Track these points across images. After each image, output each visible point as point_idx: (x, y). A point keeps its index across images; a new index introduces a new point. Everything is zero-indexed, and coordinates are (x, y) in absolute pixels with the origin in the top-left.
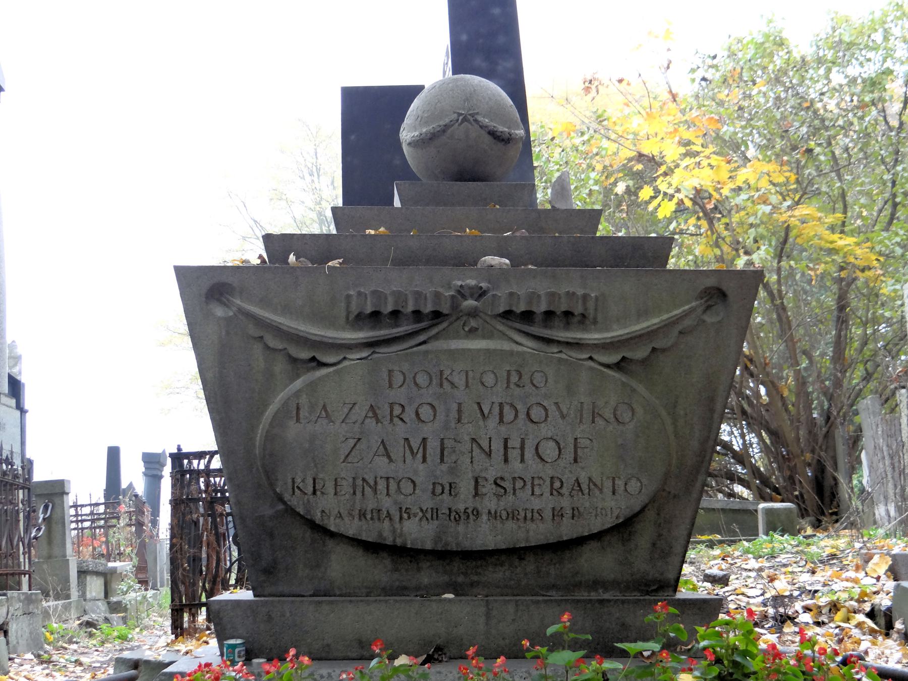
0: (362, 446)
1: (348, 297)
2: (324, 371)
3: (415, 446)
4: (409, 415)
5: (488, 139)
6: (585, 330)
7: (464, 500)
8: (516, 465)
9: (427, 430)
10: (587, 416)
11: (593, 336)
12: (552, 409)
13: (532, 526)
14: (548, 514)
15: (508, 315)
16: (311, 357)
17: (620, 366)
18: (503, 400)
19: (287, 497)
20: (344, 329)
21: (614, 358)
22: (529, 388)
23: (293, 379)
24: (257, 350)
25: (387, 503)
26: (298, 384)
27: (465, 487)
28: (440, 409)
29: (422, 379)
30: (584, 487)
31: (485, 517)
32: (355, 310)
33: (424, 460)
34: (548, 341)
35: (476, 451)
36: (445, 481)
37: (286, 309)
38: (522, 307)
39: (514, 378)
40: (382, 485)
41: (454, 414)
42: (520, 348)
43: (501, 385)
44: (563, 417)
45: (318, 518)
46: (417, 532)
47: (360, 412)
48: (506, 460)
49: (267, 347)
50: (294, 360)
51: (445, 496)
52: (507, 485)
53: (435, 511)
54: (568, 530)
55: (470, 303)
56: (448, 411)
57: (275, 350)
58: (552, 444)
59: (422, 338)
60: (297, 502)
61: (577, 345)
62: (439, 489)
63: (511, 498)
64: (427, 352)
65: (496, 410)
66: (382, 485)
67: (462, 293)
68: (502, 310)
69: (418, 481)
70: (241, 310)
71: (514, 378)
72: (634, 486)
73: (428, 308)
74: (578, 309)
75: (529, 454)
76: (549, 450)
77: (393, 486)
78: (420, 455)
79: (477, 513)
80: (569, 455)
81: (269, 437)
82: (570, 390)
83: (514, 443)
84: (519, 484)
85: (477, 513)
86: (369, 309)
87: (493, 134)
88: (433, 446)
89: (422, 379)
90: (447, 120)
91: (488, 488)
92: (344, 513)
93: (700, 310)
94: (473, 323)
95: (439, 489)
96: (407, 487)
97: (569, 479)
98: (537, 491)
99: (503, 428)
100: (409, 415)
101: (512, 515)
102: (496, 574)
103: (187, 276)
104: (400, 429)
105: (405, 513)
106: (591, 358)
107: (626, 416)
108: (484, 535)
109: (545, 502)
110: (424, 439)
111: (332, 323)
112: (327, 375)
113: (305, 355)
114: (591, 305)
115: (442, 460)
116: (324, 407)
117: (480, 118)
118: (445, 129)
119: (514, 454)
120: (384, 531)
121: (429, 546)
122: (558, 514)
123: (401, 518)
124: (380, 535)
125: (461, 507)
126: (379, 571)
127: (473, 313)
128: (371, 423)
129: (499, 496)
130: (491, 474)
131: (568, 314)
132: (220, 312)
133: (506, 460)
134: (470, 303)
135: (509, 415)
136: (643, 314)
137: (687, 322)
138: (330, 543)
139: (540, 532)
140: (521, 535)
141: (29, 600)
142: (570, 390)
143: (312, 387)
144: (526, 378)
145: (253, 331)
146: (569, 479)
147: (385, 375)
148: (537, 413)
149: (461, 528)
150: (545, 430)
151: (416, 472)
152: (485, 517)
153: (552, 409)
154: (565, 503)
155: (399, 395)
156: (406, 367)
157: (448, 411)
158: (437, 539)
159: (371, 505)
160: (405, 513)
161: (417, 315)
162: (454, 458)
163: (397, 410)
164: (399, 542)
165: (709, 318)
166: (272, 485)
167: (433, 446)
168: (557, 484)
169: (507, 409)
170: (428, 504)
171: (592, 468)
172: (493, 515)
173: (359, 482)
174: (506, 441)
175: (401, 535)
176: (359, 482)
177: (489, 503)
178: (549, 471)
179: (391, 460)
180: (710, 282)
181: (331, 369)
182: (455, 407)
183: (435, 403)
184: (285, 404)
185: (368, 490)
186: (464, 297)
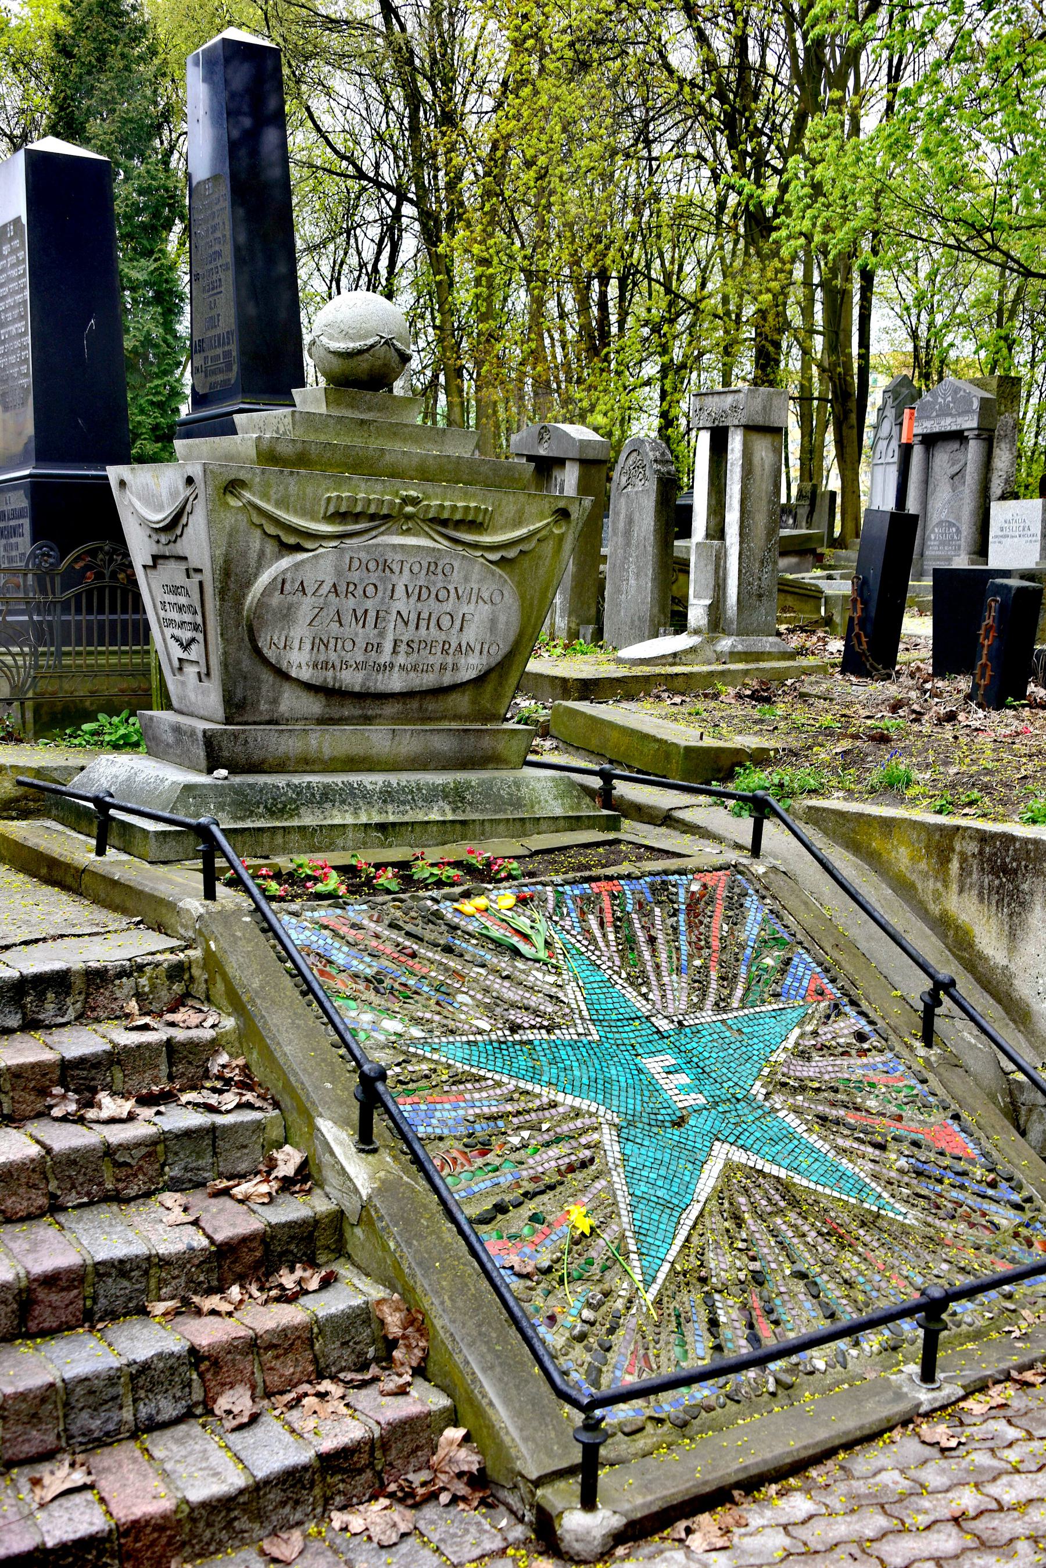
0: (323, 613)
4: (359, 592)
7: (386, 657)
8: (423, 630)
9: (369, 604)
10: (474, 598)
11: (487, 539)
12: (452, 591)
13: (425, 675)
14: (437, 667)
15: (432, 520)
17: (503, 562)
19: (265, 651)
22: (440, 576)
23: (277, 559)
24: (258, 533)
25: (333, 657)
27: (388, 646)
29: (372, 565)
32: (331, 510)
40: (332, 645)
45: (284, 666)
46: (352, 679)
52: (415, 646)
54: (447, 679)
55: (409, 509)
60: (270, 654)
61: (475, 546)
66: (332, 641)
67: (406, 501)
72: (494, 649)
76: (446, 621)
81: (260, 604)
82: (466, 579)
83: (425, 615)
85: (392, 665)
86: (343, 510)
88: (371, 615)
89: (372, 565)
90: (370, 341)
91: (403, 648)
96: (349, 645)
101: (415, 668)
102: (390, 709)
104: (351, 603)
107: (497, 598)
108: (396, 683)
109: (436, 659)
111: (313, 519)
113: (292, 540)
119: (423, 624)
120: (328, 677)
121: (357, 689)
122: (443, 667)
125: (382, 661)
126: (314, 706)
127: (409, 517)
128: (332, 596)
132: (233, 502)
134: (409, 509)
135: (424, 596)
136: (517, 523)
137: (543, 533)
138: (287, 687)
139: (428, 680)
140: (418, 681)
142: (466, 579)
143: (297, 566)
145: (256, 519)
148: (443, 594)
149: (380, 677)
150: (448, 607)
153: (452, 591)
155: (355, 576)
156: (363, 555)
158: (363, 684)
159: (322, 658)
161: (373, 517)
163: (351, 588)
166: (253, 640)
167: (371, 615)
170: (360, 658)
171: (470, 635)
172: (402, 668)
177: (401, 659)
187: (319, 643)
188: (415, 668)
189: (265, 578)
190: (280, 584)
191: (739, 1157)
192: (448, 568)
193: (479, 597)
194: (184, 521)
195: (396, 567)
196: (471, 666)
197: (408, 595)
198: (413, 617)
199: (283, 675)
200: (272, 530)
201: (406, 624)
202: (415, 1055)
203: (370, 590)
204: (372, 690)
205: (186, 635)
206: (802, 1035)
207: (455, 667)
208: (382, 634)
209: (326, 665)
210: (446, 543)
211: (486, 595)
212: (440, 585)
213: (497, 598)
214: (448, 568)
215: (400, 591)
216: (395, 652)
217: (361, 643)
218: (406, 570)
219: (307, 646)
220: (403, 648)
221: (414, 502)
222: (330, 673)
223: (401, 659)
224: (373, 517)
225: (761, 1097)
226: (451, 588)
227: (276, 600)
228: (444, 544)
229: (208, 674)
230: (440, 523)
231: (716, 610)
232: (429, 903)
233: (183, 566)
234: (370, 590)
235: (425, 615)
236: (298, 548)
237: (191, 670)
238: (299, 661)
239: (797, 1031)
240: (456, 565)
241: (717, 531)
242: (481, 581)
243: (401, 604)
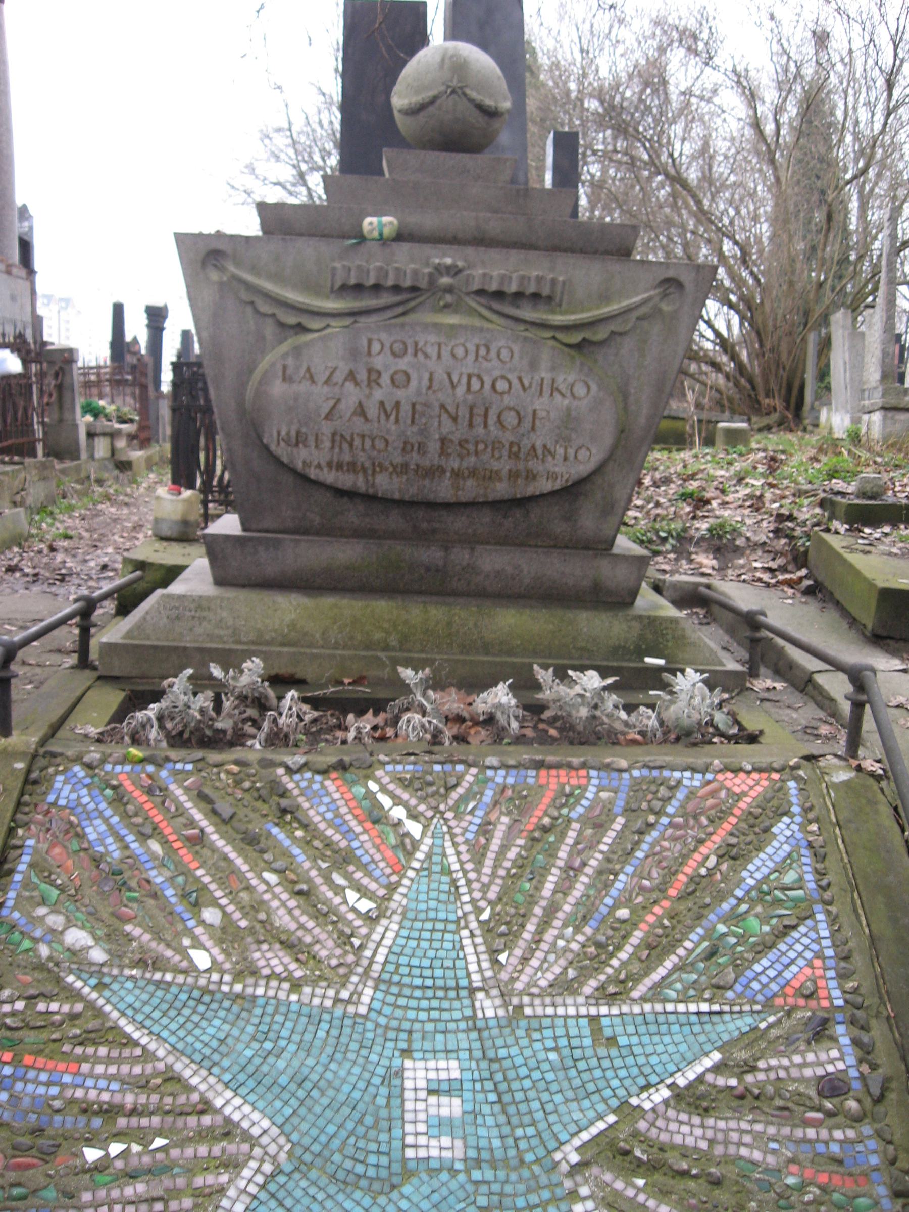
1: (334, 269)
2: (310, 337)
3: (389, 408)
5: (476, 113)
6: (553, 312)
9: (400, 394)
11: (558, 319)
14: (504, 473)
15: (481, 292)
16: (295, 324)
17: (578, 347)
18: (470, 371)
19: (273, 448)
20: (328, 298)
22: (495, 362)
25: (362, 458)
26: (284, 347)
27: (434, 447)
28: (414, 376)
30: (540, 452)
31: (448, 474)
32: (338, 284)
33: (397, 421)
35: (445, 416)
36: (414, 440)
37: (277, 277)
38: (494, 287)
39: (483, 351)
40: (357, 442)
41: (425, 382)
42: (490, 326)
43: (471, 357)
44: (524, 389)
45: (299, 466)
47: (339, 377)
48: (471, 425)
49: (256, 311)
50: (282, 325)
51: (414, 454)
52: (471, 447)
53: (405, 466)
55: (445, 280)
56: (420, 379)
57: (265, 315)
58: (513, 413)
59: (400, 310)
61: (544, 326)
62: (409, 448)
63: (473, 459)
64: (403, 325)
65: (464, 380)
67: (442, 270)
68: (475, 287)
69: (391, 439)
70: (235, 277)
71: (483, 351)
73: (407, 283)
74: (546, 292)
77: (368, 443)
78: (393, 417)
80: (527, 424)
82: (533, 365)
83: (479, 411)
84: (481, 447)
85: (443, 471)
86: (353, 281)
87: (480, 107)
88: (406, 408)
92: (323, 463)
93: (657, 299)
94: (449, 298)
95: (409, 448)
96: (380, 445)
98: (497, 454)
99: (470, 397)
103: (184, 241)
106: (554, 338)
107: (580, 390)
112: (312, 341)
113: (292, 320)
114: (559, 288)
115: (413, 422)
116: (308, 370)
117: (468, 91)
118: (433, 101)
119: (478, 420)
121: (397, 496)
122: (514, 475)
123: (374, 471)
124: (355, 484)
127: (449, 290)
128: (349, 386)
129: (462, 457)
130: (456, 437)
131: (536, 296)
132: (214, 276)
133: (471, 425)
141: (44, 466)
144: (493, 354)
145: (245, 295)
147: (365, 343)
148: (501, 386)
151: (388, 431)
152: (448, 474)
153: (515, 382)
157: (420, 379)
159: (347, 457)
161: (397, 289)
162: (424, 420)
164: (371, 491)
165: (666, 307)
166: (260, 439)
168: (515, 449)
169: (474, 380)
170: (398, 459)
172: (456, 474)
173: (338, 438)
174: (471, 408)
175: (373, 485)
176: (338, 438)
177: (454, 463)
178: (508, 437)
179: (366, 419)
180: (671, 274)
181: (316, 335)
182: (426, 376)
183: (410, 371)
184: (273, 365)
185: (345, 446)
186: (441, 274)
192: (505, 354)
193: (554, 389)
195: (432, 351)
197: (454, 387)
198: (463, 412)
200: (265, 308)
201: (455, 419)
206: (717, 1069)
211: (563, 387)
212: (497, 373)
213: (580, 390)
214: (505, 354)
216: (443, 452)
218: (445, 353)
219: (327, 444)
225: (564, 1167)
232: (281, 771)
235: (479, 411)
236: (300, 328)
239: (716, 1056)
240: (516, 349)
242: (553, 369)
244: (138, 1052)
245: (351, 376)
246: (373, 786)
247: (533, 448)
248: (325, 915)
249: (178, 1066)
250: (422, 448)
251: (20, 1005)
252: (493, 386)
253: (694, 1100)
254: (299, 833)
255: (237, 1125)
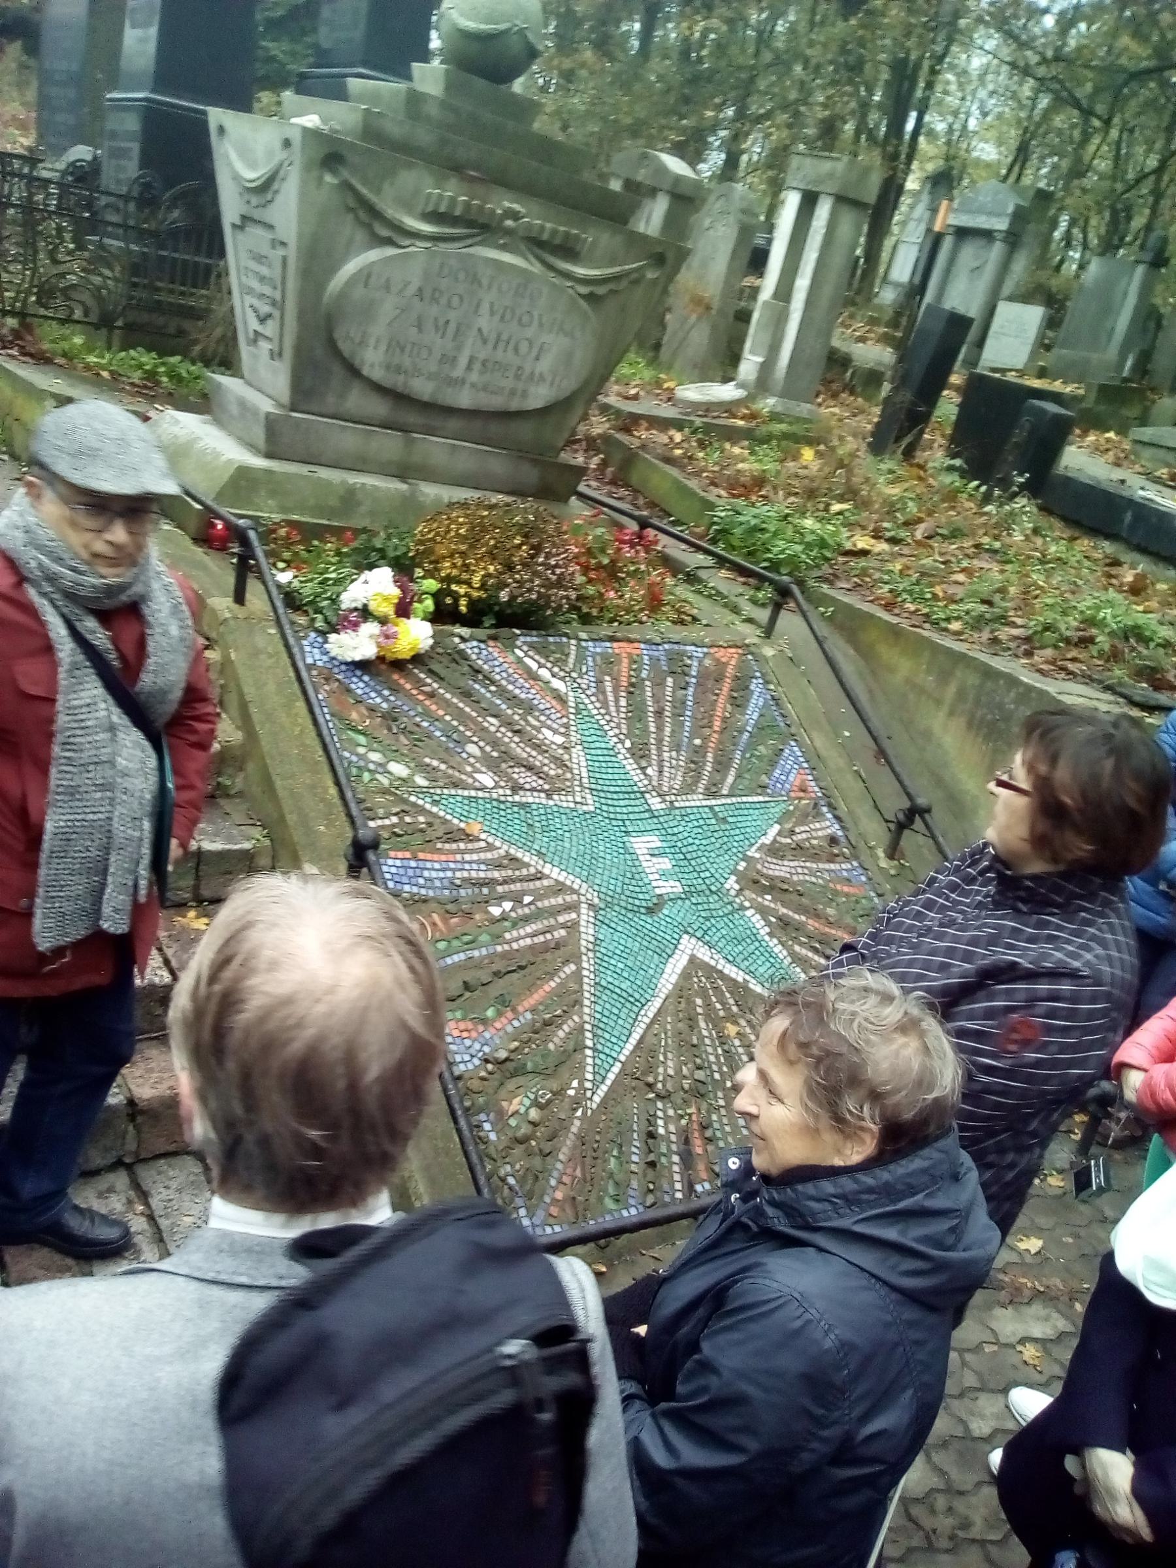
4: (443, 301)
6: (575, 264)
7: (458, 372)
9: (452, 315)
11: (580, 271)
21: (584, 290)
25: (407, 362)
27: (463, 361)
29: (462, 276)
32: (430, 209)
34: (551, 268)
40: (408, 350)
45: (357, 363)
46: (423, 388)
47: (412, 289)
48: (495, 347)
54: (514, 405)
55: (509, 223)
59: (469, 242)
60: (345, 347)
61: (568, 276)
75: (511, 347)
79: (463, 381)
80: (534, 353)
81: (343, 294)
83: (504, 337)
88: (452, 327)
89: (462, 276)
90: (502, 27)
91: (477, 366)
97: (528, 370)
100: (443, 301)
101: (485, 388)
102: (454, 424)
104: (434, 310)
105: (417, 372)
108: (465, 399)
110: (448, 322)
119: (501, 345)
120: (397, 382)
122: (513, 393)
126: (379, 407)
127: (509, 232)
128: (416, 300)
130: (482, 356)
132: (329, 178)
134: (509, 223)
135: (508, 317)
139: (496, 402)
145: (351, 202)
146: (528, 370)
148: (525, 319)
150: (530, 332)
154: (520, 386)
159: (396, 361)
160: (417, 372)
167: (452, 327)
172: (473, 385)
177: (474, 377)
187: (396, 345)
188: (485, 388)
189: (351, 267)
190: (365, 276)
191: (704, 954)
194: (275, 186)
195: (485, 282)
196: (539, 396)
199: (354, 372)
201: (485, 342)
202: (414, 805)
203: (456, 300)
204: (440, 402)
205: (265, 309)
206: (779, 834)
207: (525, 395)
208: (459, 348)
209: (399, 369)
210: (538, 265)
215: (485, 308)
216: (469, 368)
217: (437, 355)
220: (477, 366)
221: (515, 216)
222: (401, 378)
223: (474, 377)
224: (470, 224)
225: (733, 893)
226: (536, 314)
227: (359, 292)
228: (536, 268)
229: (280, 354)
230: (537, 244)
231: (766, 368)
232: (457, 640)
233: (269, 236)
234: (455, 301)
235: (504, 337)
236: (389, 242)
237: (265, 346)
238: (373, 362)
239: (777, 827)
241: (784, 292)
243: (484, 322)
244: (483, 844)
245: (420, 293)
246: (520, 654)
247: (532, 373)
248: (539, 747)
249: (512, 851)
250: (454, 361)
251: (395, 819)
252: (520, 320)
253: (774, 851)
254: (493, 688)
255: (563, 884)
